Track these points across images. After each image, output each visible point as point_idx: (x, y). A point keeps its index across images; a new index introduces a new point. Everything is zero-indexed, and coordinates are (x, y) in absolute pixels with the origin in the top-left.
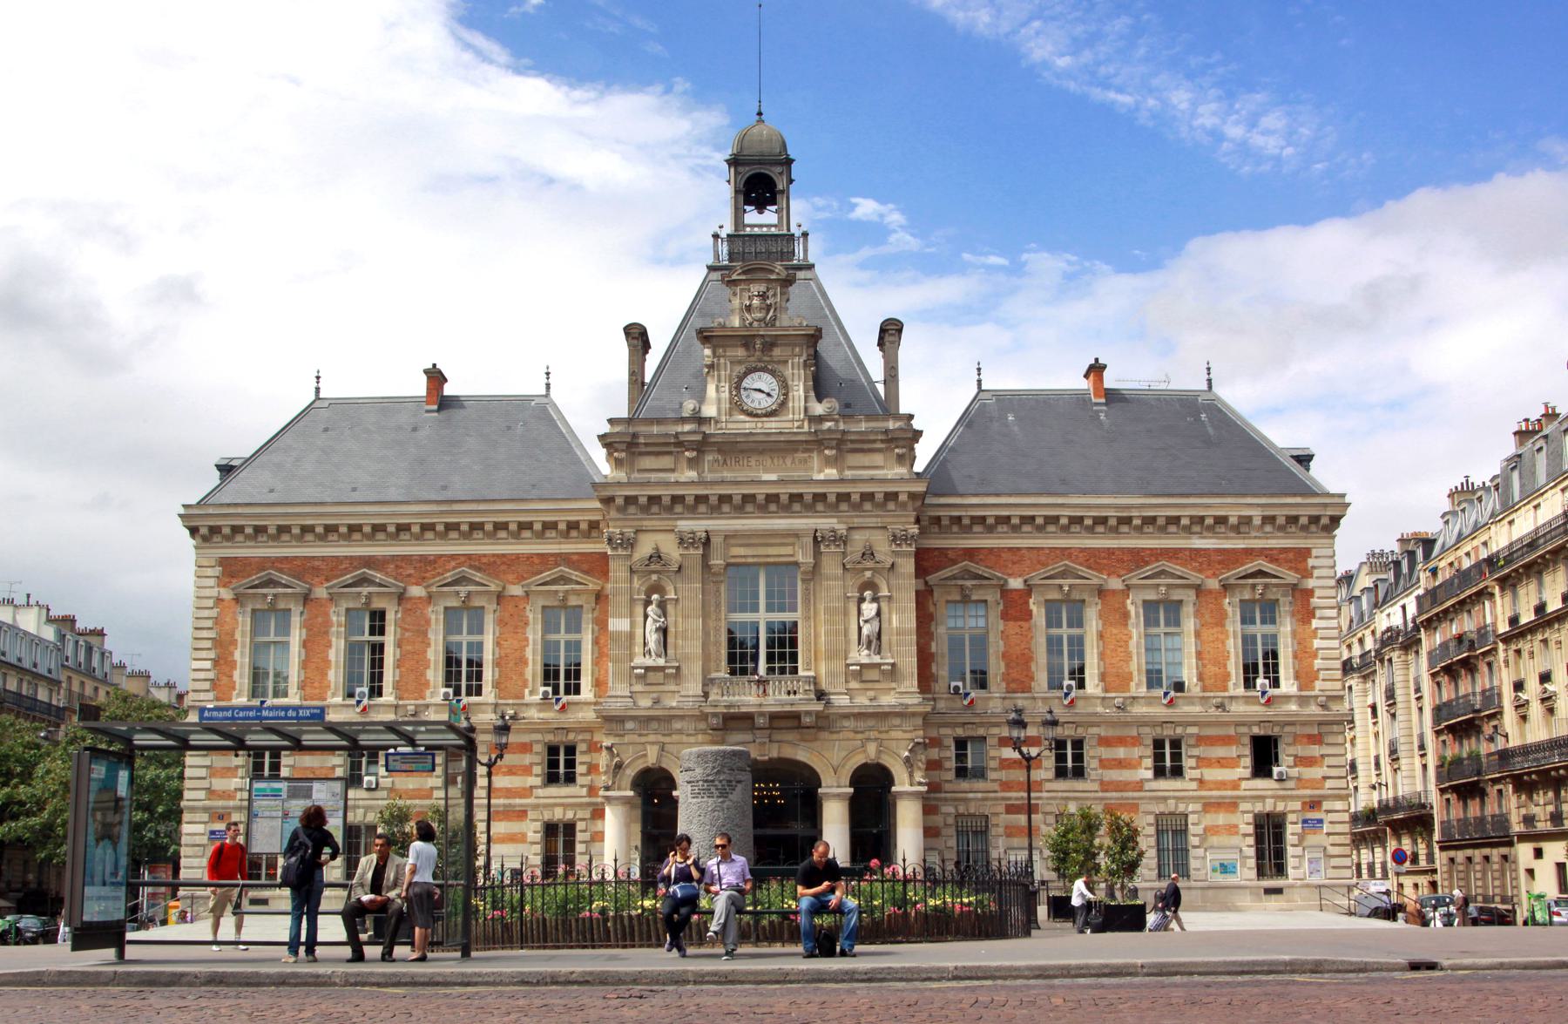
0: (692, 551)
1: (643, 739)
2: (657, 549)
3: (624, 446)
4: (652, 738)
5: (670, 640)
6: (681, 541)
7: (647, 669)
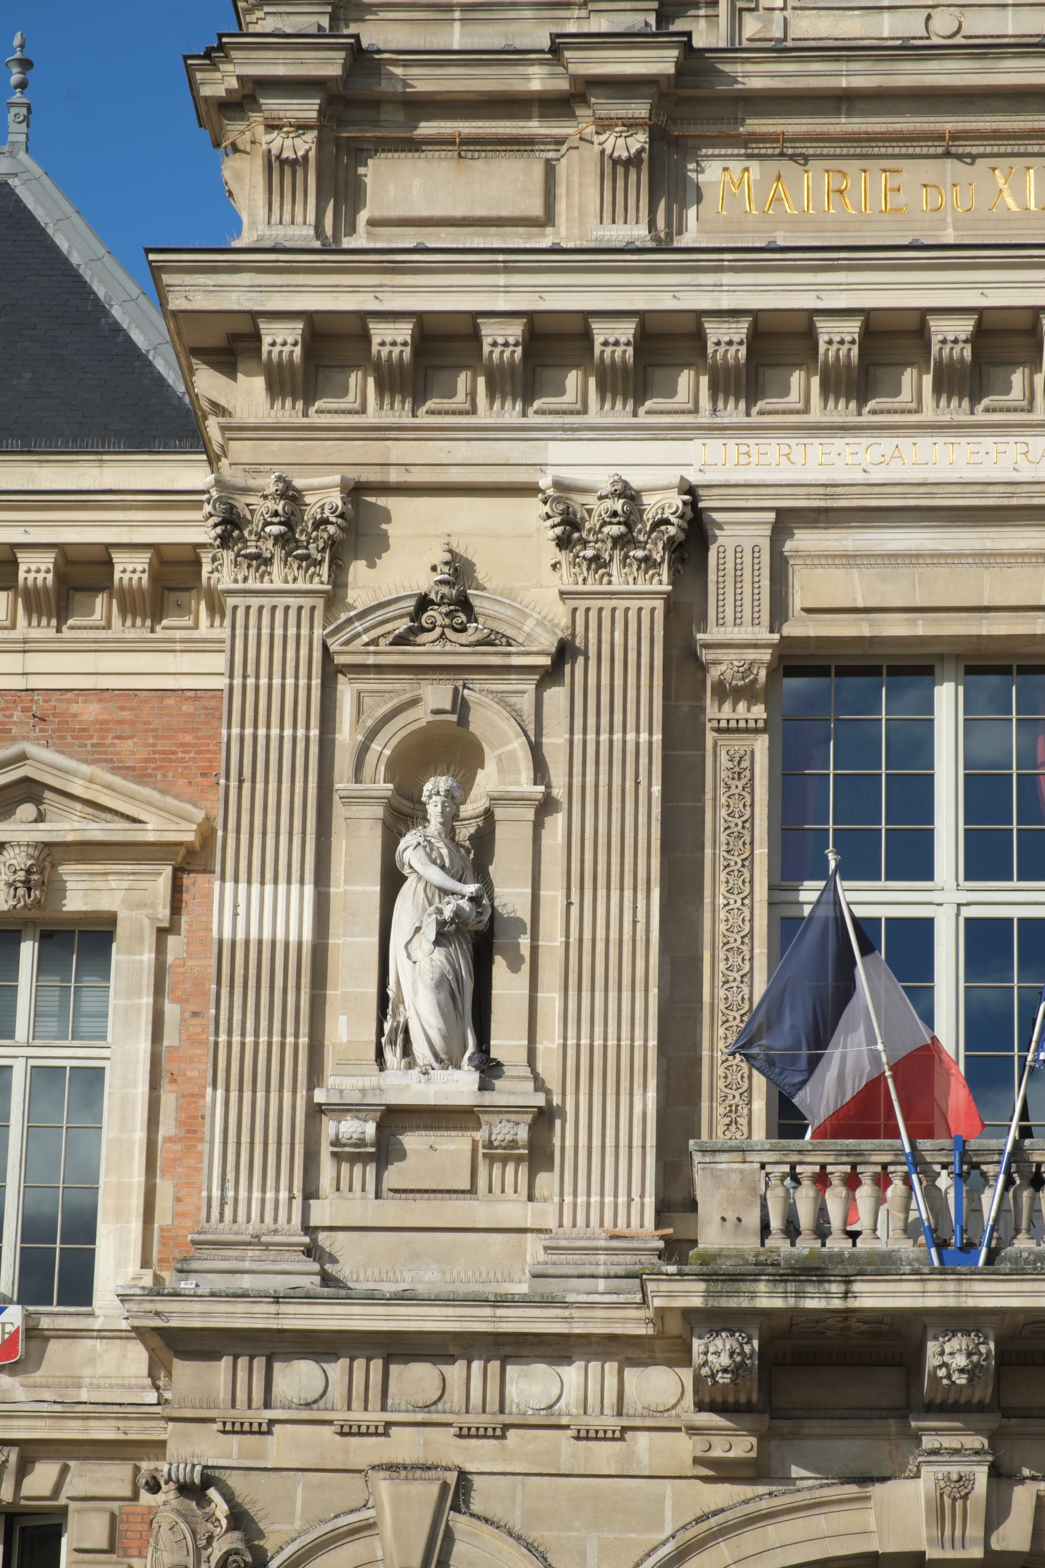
0: (619, 578)
1: (367, 1451)
2: (459, 570)
3: (308, 108)
4: (404, 1445)
5: (507, 986)
6: (570, 531)
7: (395, 1119)
